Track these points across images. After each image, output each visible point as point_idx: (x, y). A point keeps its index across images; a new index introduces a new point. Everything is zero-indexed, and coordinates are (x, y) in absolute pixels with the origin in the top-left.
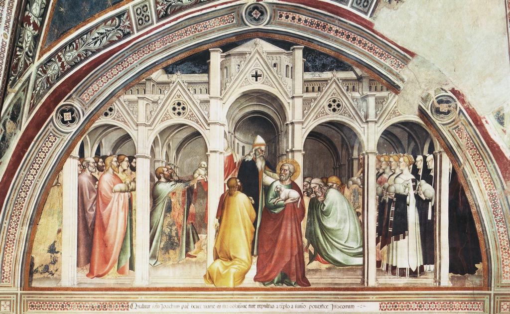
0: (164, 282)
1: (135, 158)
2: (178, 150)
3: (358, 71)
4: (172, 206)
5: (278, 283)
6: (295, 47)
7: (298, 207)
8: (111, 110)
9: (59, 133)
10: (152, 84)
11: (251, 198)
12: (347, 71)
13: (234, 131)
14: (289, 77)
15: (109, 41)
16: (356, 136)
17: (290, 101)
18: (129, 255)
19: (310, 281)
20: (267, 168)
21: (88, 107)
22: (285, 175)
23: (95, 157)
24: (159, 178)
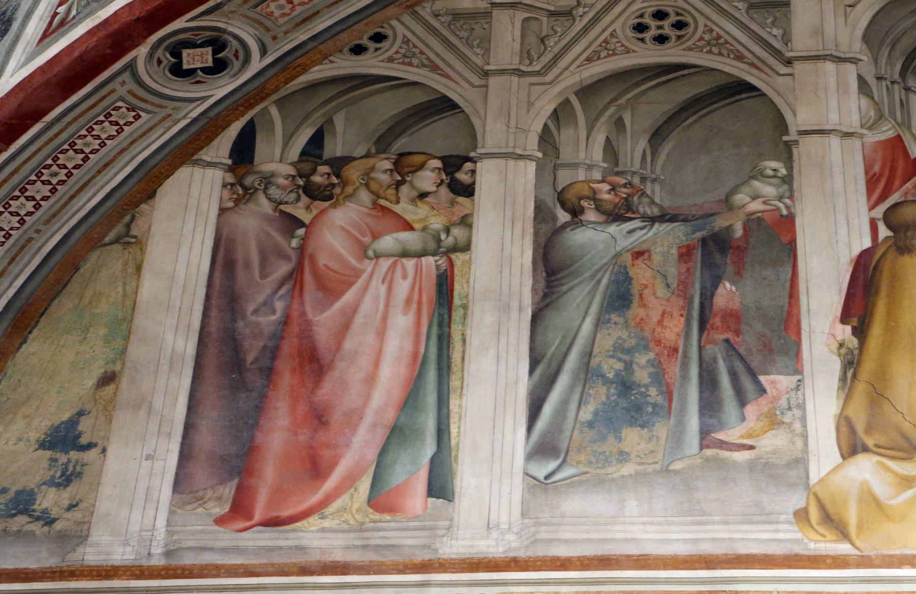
0: (594, 536)
1: (473, 161)
2: (657, 136)
4: (635, 290)
8: (378, 38)
9: (157, 100)
13: (903, 73)
18: (429, 449)
21: (286, 33)
23: (299, 161)
24: (576, 212)
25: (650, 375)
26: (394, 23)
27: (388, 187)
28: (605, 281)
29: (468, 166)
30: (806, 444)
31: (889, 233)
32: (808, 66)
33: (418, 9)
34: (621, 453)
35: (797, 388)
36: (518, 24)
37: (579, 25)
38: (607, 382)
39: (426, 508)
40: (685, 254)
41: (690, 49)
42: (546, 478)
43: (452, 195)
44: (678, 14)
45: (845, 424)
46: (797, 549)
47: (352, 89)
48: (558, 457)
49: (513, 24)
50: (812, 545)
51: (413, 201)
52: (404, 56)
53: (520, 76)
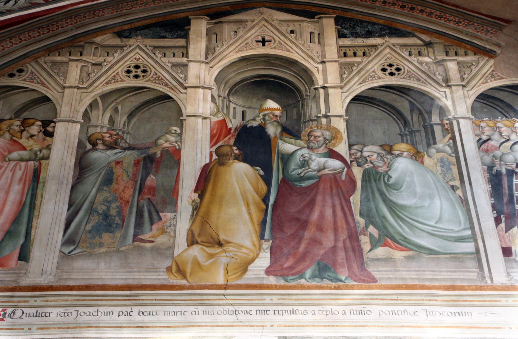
0: (85, 277)
2: (131, 115)
3: (424, 37)
4: (115, 177)
5: (313, 277)
6: (321, 16)
7: (343, 178)
8: (21, 71)
10: (94, 47)
11: (258, 168)
12: (407, 37)
14: (315, 43)
15: (30, 3)
16: (432, 99)
17: (320, 66)
18: (22, 241)
19: (376, 275)
20: (285, 135)
22: (317, 142)
25: (116, 211)
26: (28, 65)
27: (18, 132)
28: (103, 173)
29: (52, 124)
30: (174, 241)
31: (217, 157)
32: (193, 90)
33: (38, 60)
34: (101, 243)
35: (174, 218)
36: (79, 68)
37: (104, 70)
38: (99, 214)
39: (17, 265)
40: (137, 163)
41: (147, 81)
42: (69, 253)
43: (44, 136)
44: (144, 67)
45: (190, 232)
46: (166, 283)
47: (7, 91)
48: (74, 245)
49: (77, 68)
50: (172, 281)
51: (27, 138)
52: (31, 79)
53: (78, 89)
